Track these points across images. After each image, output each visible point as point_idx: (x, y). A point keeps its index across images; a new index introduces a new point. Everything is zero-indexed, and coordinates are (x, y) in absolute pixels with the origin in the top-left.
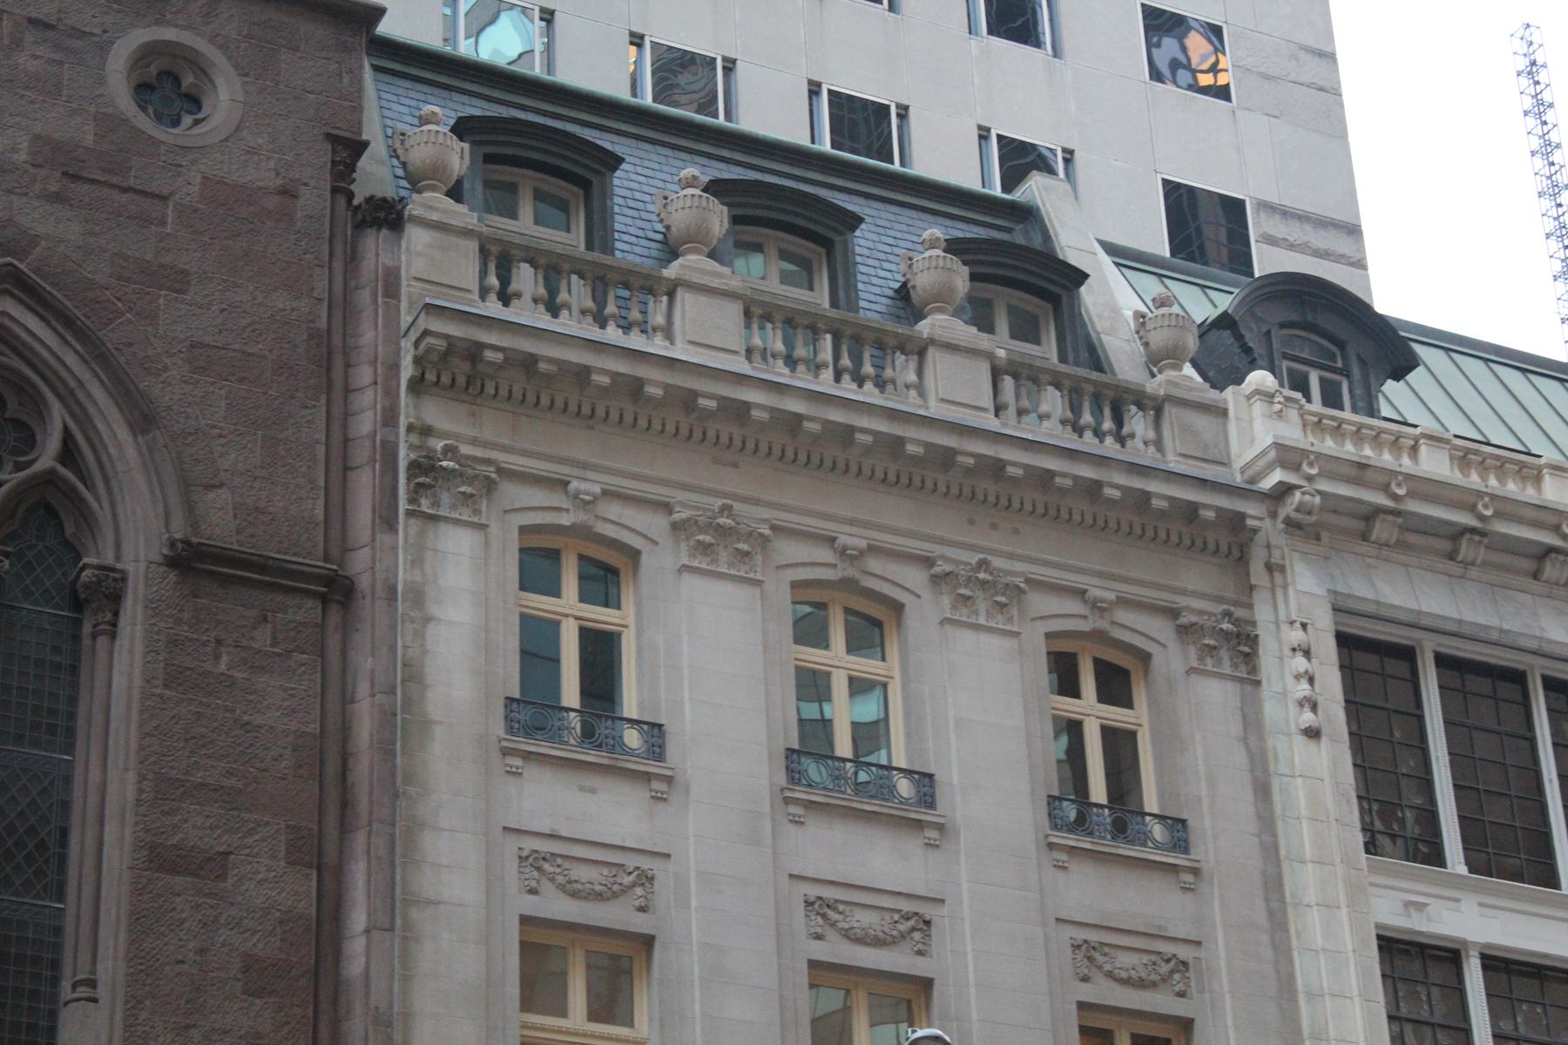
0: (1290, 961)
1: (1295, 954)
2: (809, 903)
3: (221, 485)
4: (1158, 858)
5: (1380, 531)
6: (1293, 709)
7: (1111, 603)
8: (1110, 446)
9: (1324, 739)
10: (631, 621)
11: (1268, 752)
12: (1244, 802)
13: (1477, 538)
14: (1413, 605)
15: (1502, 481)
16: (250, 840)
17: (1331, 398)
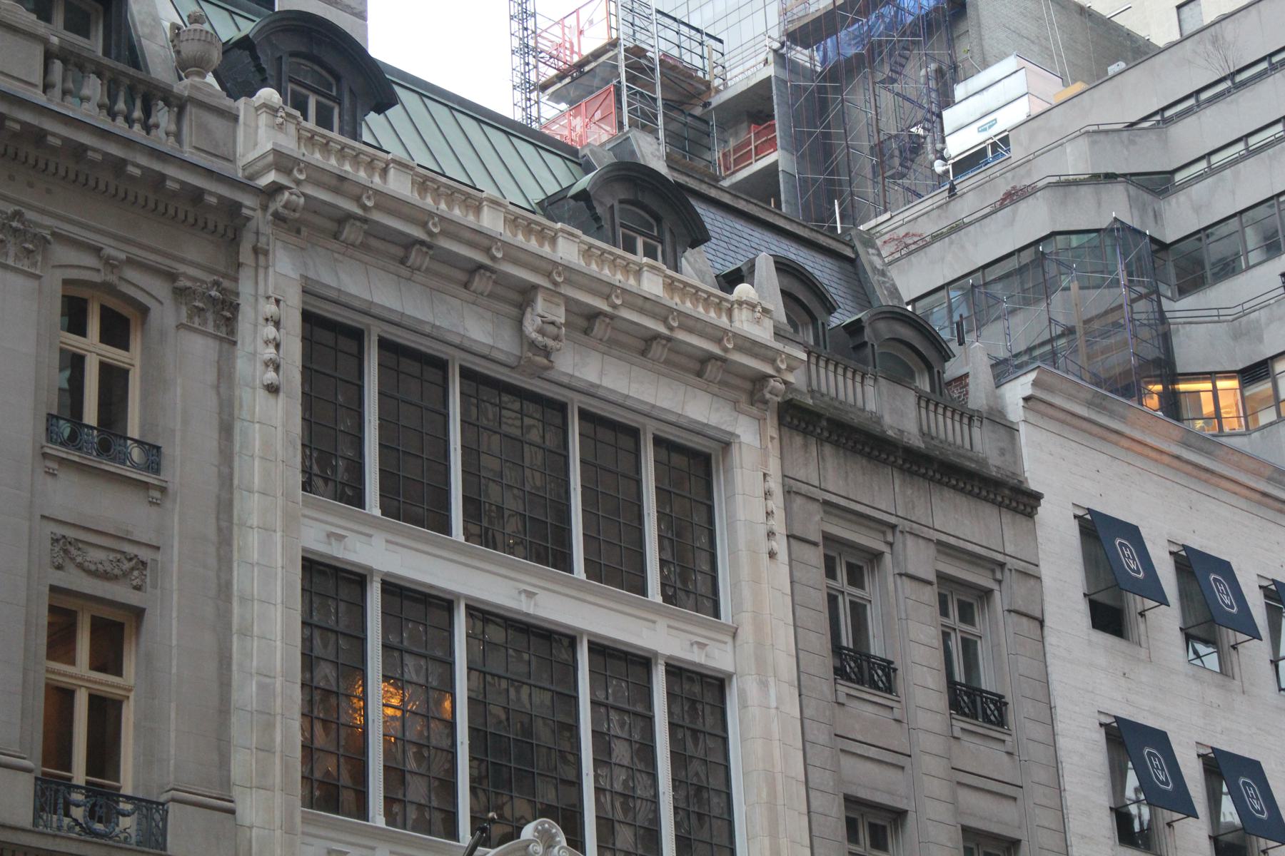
0: (230, 569)
1: (235, 565)
4: (134, 476)
5: (657, 350)
6: (260, 367)
7: (121, 262)
8: (137, 132)
9: (281, 395)
10: (137, 363)
11: (236, 399)
12: (209, 439)
13: (425, 249)
14: (368, 297)
15: (450, 206)
17: (324, 120)
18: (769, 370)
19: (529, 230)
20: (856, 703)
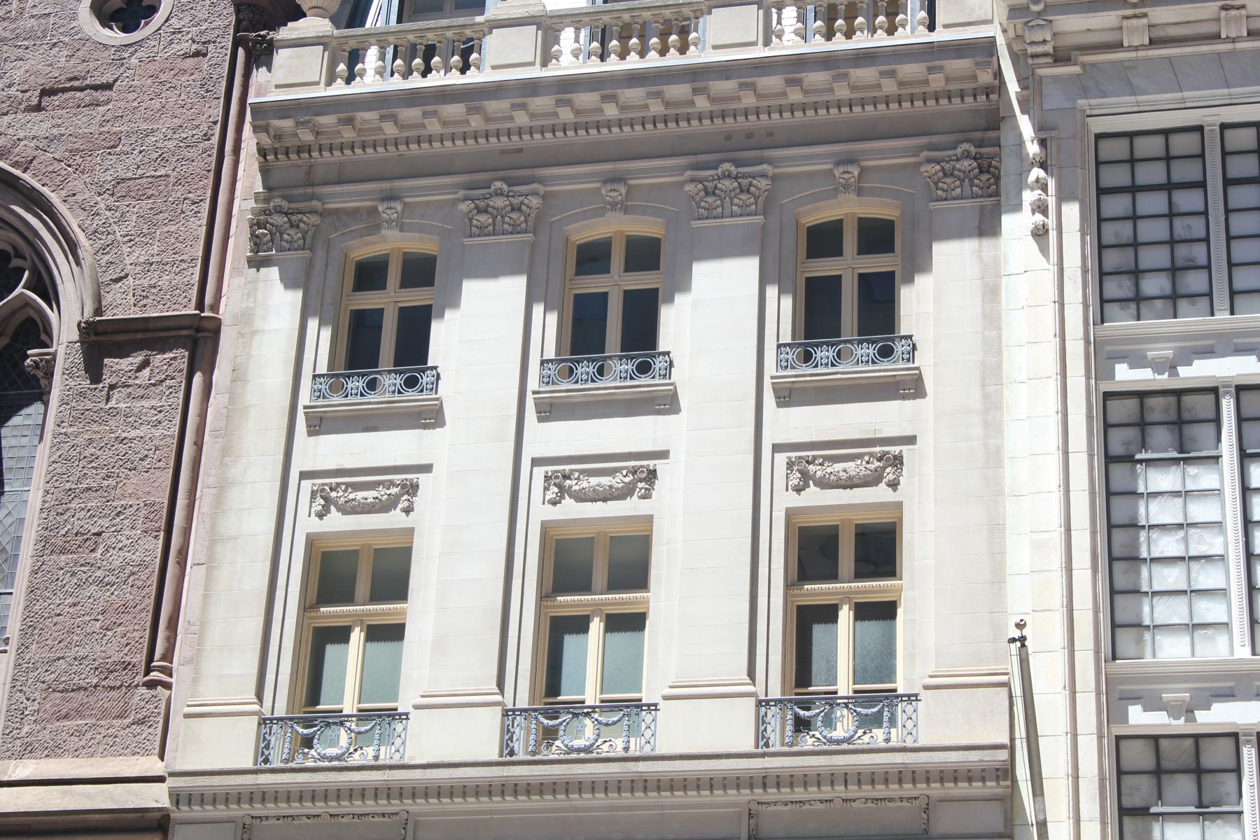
2: (547, 478)
3: (127, 276)
16: (118, 520)
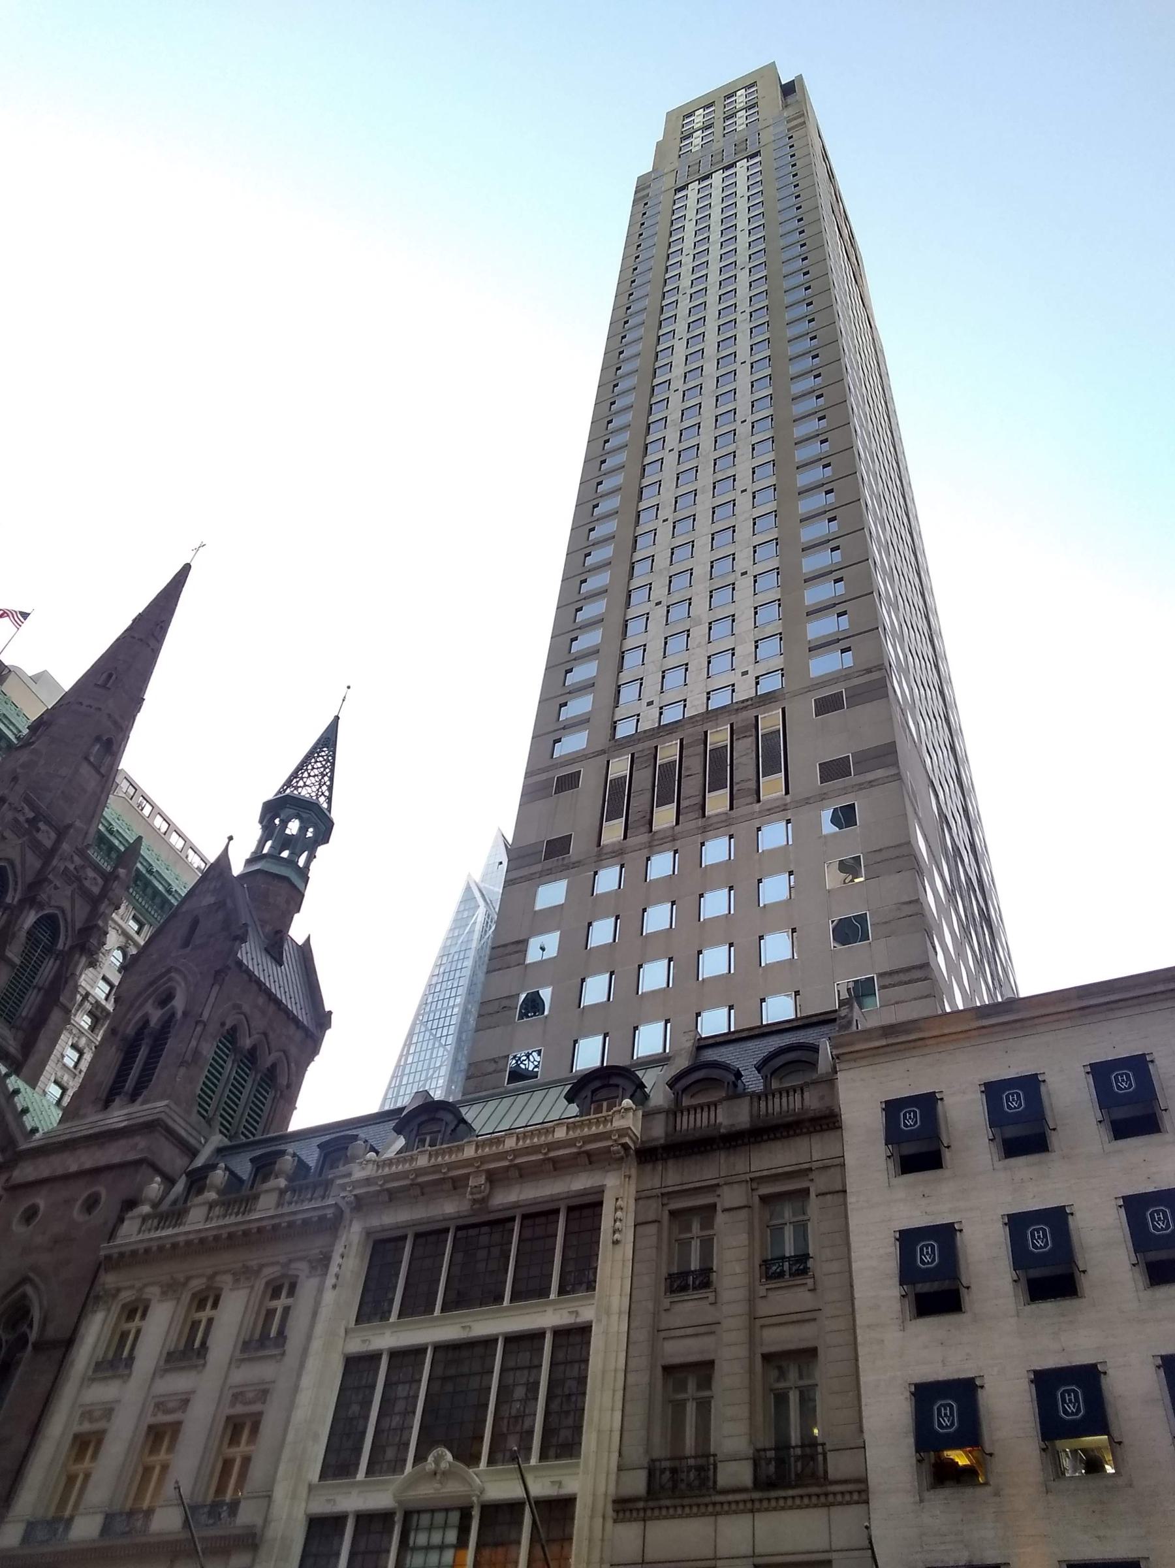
18: (610, 1143)
19: (405, 1160)
20: (680, 1305)
